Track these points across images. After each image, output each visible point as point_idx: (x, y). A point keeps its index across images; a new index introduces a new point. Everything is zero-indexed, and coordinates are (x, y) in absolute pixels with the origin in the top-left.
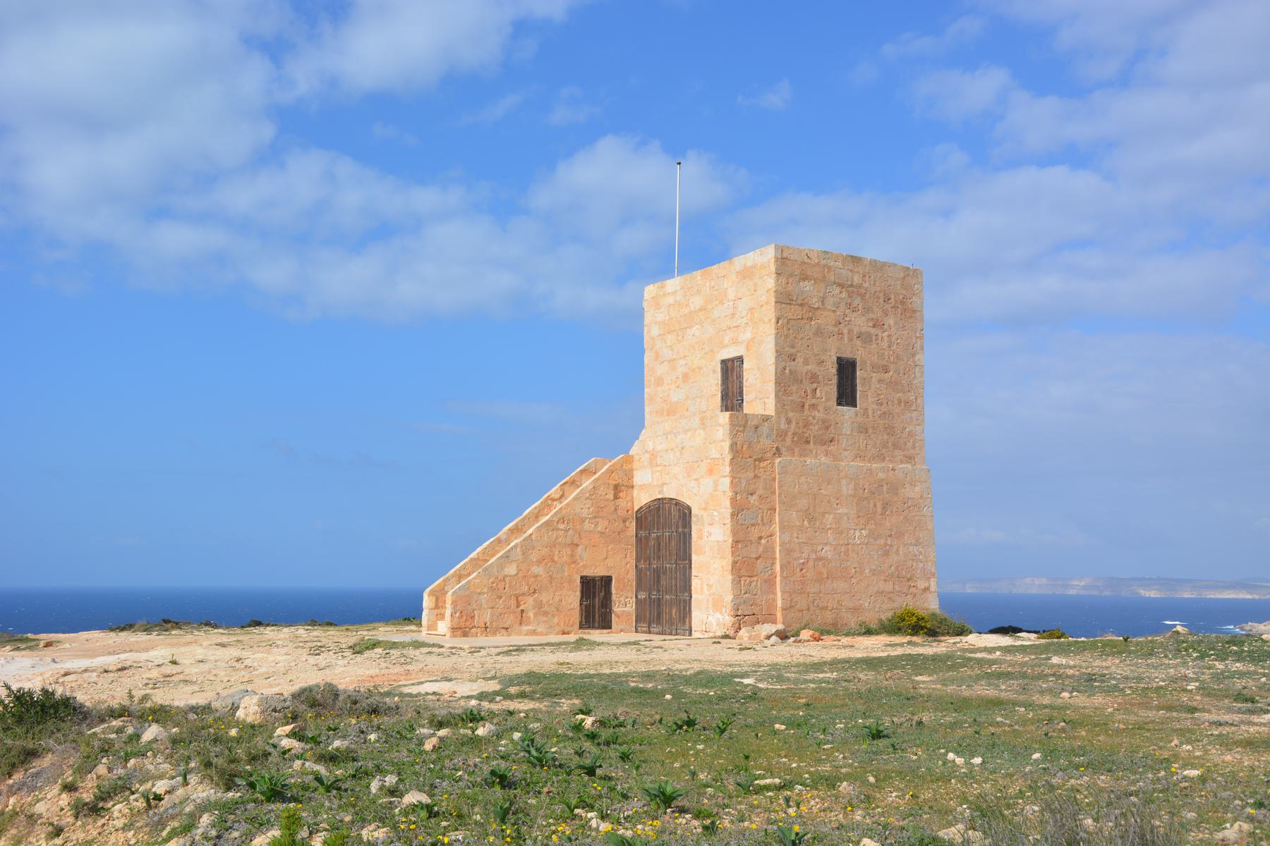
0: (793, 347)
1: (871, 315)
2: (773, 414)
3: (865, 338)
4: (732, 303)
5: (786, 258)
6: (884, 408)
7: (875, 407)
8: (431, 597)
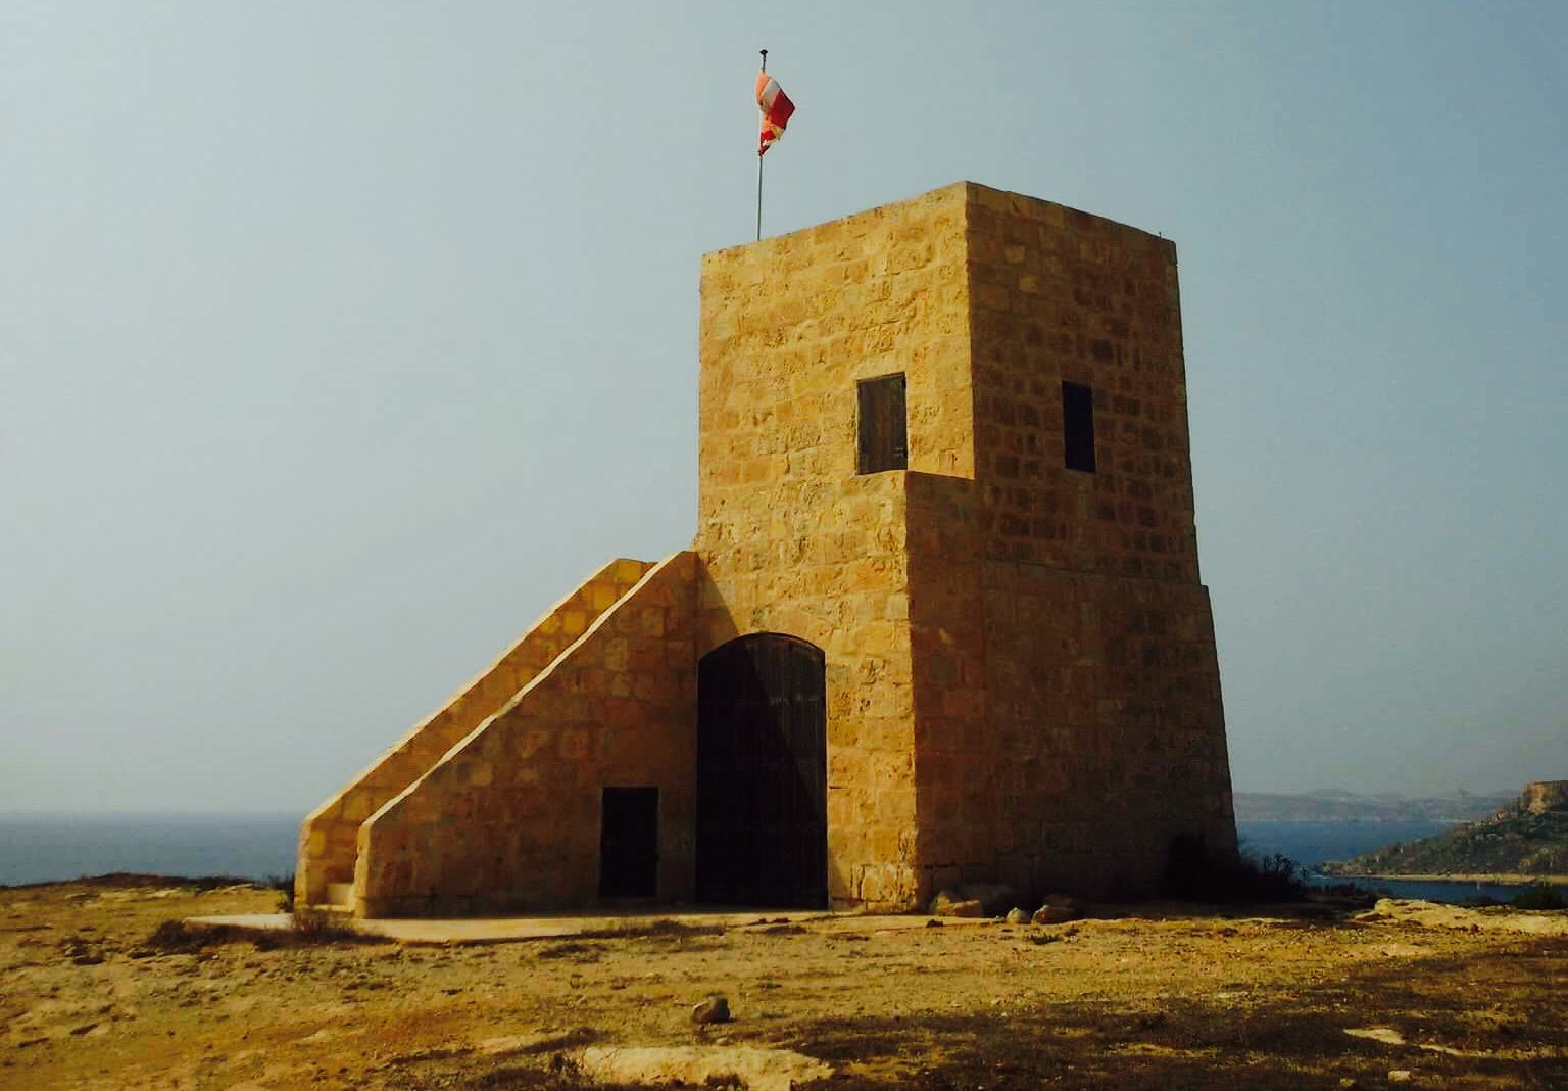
2: (972, 478)
3: (1102, 351)
4: (881, 281)
8: (320, 836)
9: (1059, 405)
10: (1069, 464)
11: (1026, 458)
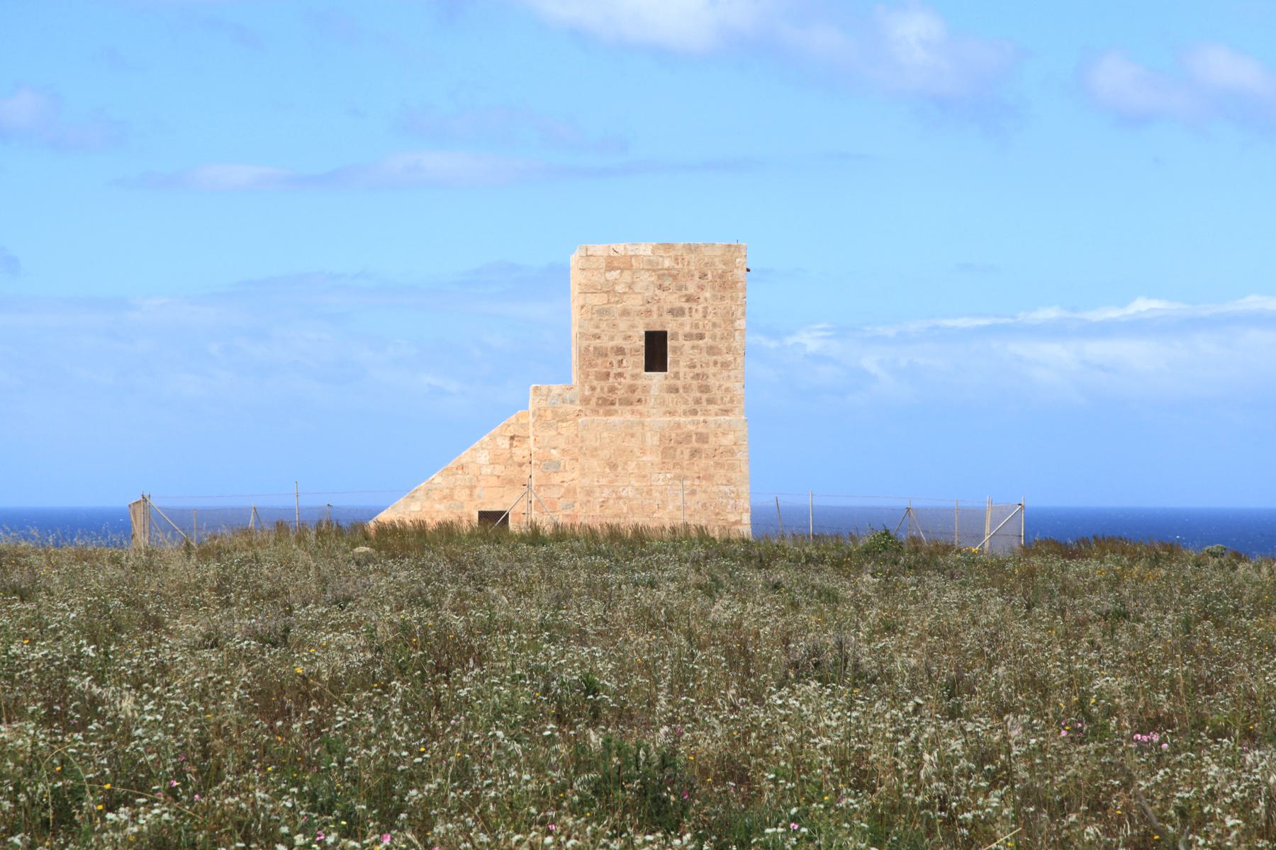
0: (597, 327)
1: (684, 292)
3: (676, 312)
5: (591, 256)
6: (697, 370)
7: (687, 370)
9: (643, 343)
10: (649, 368)
11: (616, 370)
